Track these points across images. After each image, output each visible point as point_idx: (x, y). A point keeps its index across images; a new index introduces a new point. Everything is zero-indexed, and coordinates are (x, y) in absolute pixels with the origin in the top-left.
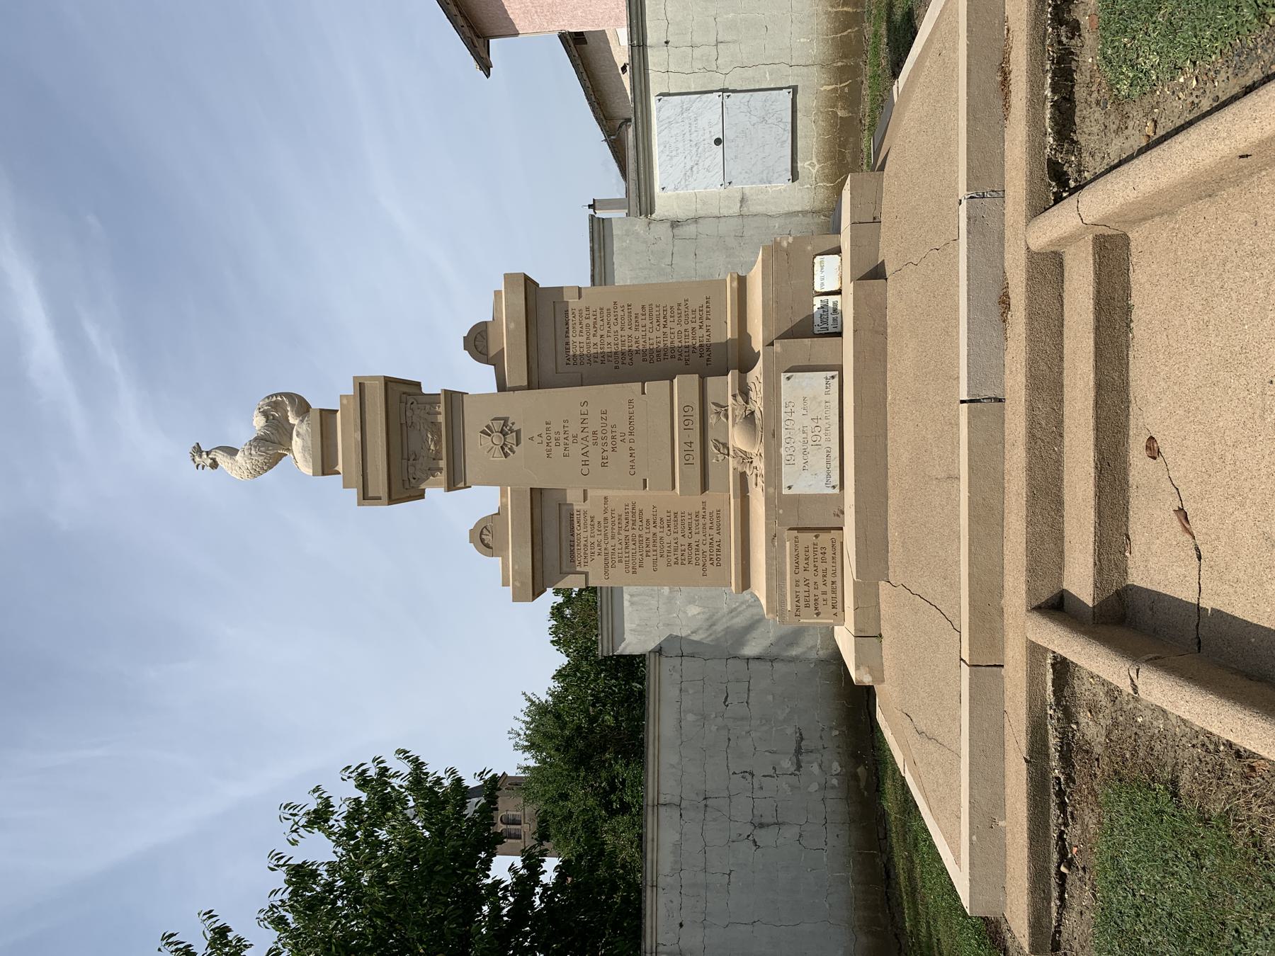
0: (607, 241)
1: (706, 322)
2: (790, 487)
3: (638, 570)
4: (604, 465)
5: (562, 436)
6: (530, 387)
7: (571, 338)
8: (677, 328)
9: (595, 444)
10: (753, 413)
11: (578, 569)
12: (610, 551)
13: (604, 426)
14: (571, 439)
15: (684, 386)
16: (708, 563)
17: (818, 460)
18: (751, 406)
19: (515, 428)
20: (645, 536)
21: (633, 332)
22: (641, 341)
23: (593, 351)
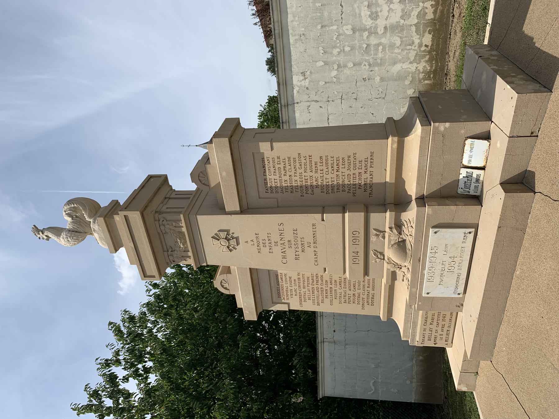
1: (369, 169)
2: (428, 293)
3: (321, 304)
4: (296, 259)
5: (267, 242)
7: (268, 177)
9: (290, 247)
10: (404, 241)
11: (283, 301)
12: (303, 294)
13: (296, 238)
14: (273, 244)
16: (366, 304)
17: (450, 280)
19: (235, 235)
20: (324, 288)
21: (313, 174)
22: (320, 180)
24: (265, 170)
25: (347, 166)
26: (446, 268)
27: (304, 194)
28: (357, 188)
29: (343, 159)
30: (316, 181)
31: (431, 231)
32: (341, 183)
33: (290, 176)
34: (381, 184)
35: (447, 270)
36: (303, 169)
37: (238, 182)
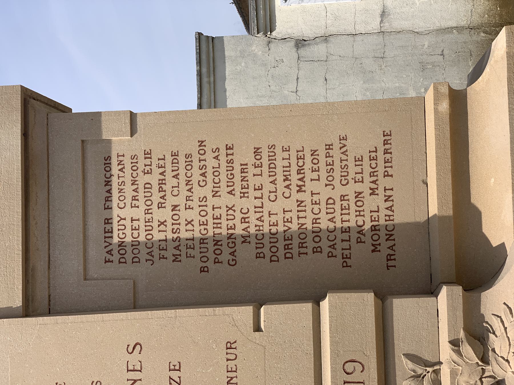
0: (218, 63)
1: (383, 182)
6: (28, 310)
7: (116, 212)
8: (325, 193)
15: (345, 313)
21: (236, 201)
22: (253, 217)
23: (158, 236)
24: (109, 191)
25: (323, 174)
27: (210, 264)
28: (353, 240)
29: (314, 153)
30: (244, 220)
32: (309, 226)
33: (175, 207)
34: (416, 225)
36: (210, 185)
37: (32, 222)
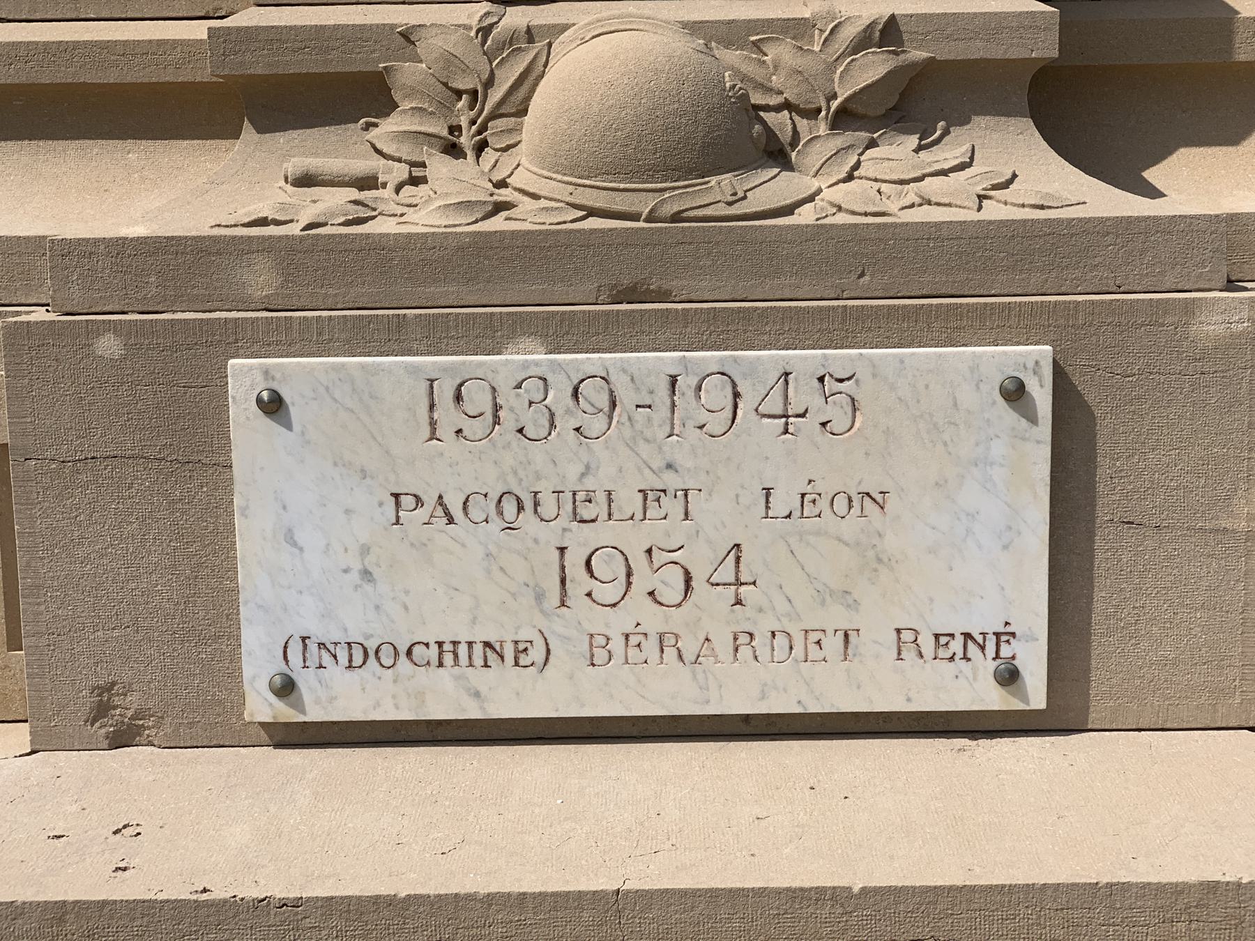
2: (273, 406)
10: (778, 154)
17: (460, 586)
18: (820, 144)
26: (603, 533)
31: (1032, 358)
35: (580, 540)
